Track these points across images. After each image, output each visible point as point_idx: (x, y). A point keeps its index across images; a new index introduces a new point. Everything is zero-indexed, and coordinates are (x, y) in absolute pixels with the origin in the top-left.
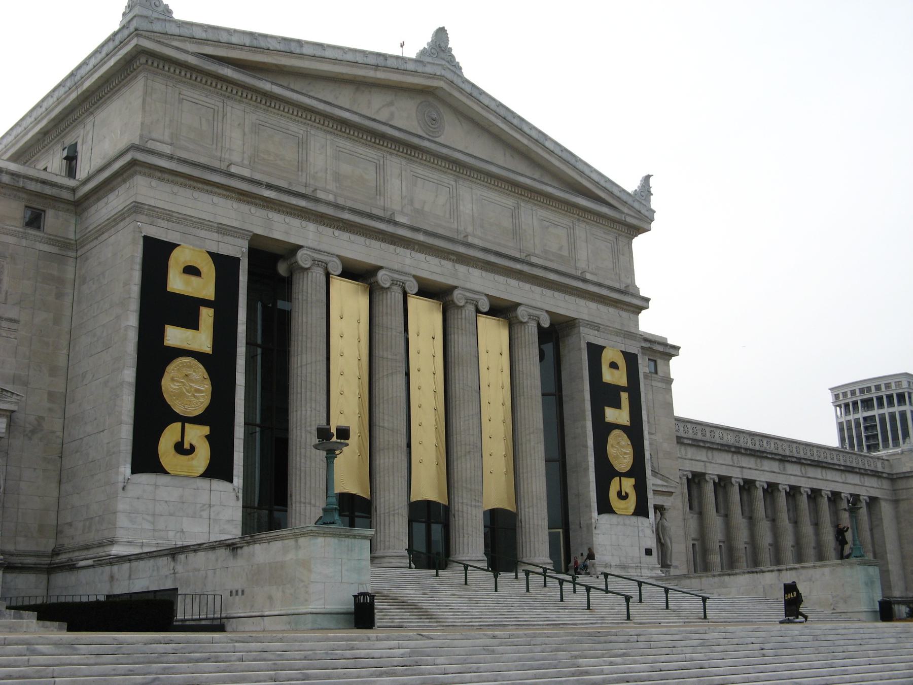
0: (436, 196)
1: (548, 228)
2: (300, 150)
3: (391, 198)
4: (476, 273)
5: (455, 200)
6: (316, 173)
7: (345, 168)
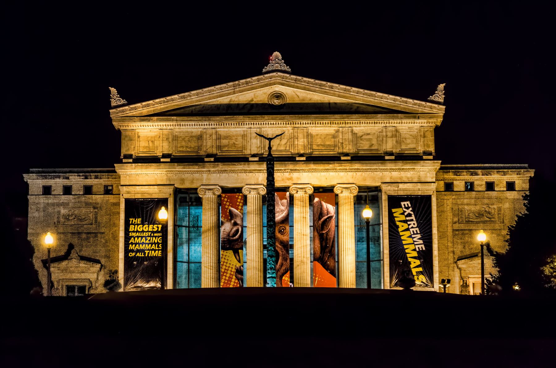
0: (280, 141)
1: (362, 136)
2: (199, 141)
3: (250, 150)
4: (305, 174)
5: (292, 140)
6: (207, 149)
7: (224, 142)
